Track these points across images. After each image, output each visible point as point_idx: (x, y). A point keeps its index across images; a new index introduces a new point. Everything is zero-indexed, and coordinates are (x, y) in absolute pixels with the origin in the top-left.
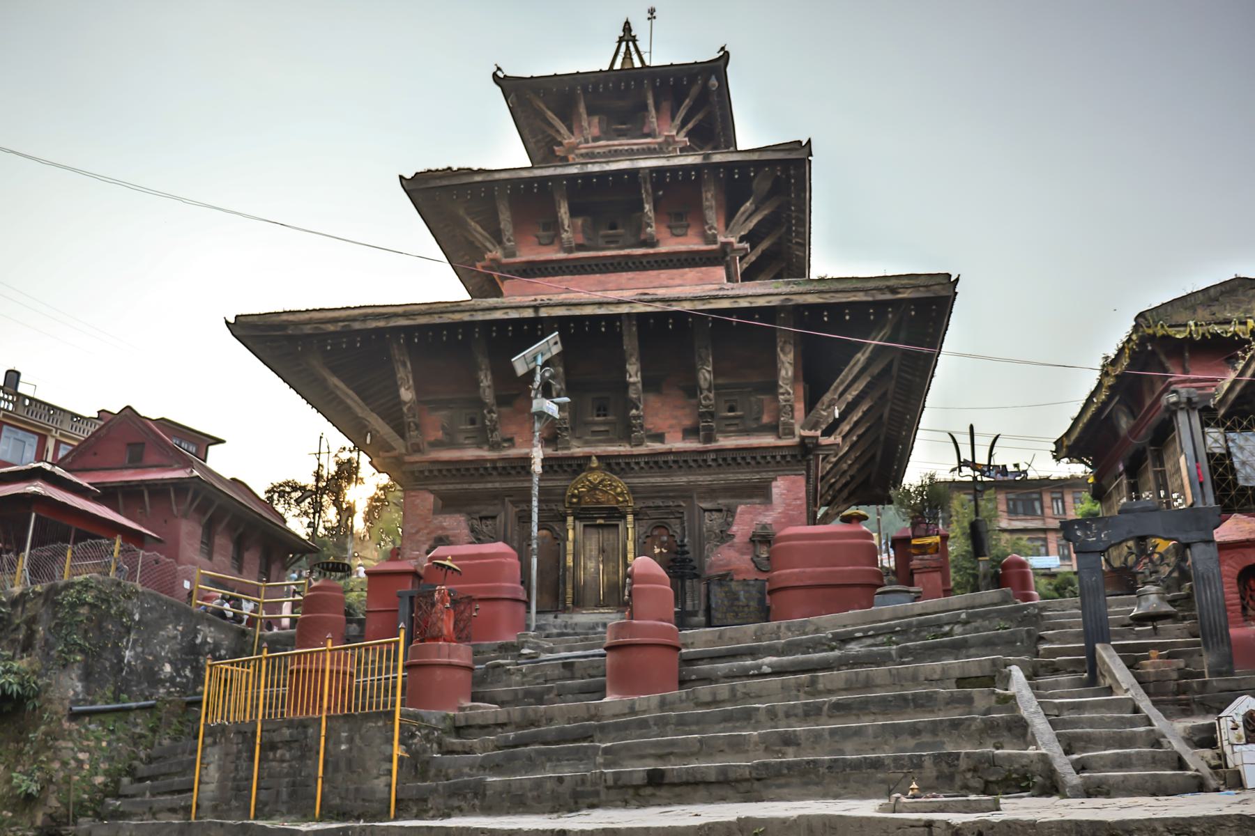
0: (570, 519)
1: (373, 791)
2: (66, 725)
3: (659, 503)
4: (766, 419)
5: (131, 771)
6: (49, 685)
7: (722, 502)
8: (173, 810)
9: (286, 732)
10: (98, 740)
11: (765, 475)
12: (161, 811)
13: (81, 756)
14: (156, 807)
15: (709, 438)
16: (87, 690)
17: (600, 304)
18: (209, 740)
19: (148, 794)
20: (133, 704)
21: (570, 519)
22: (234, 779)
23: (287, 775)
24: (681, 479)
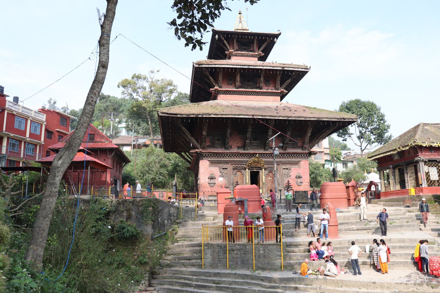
0: (247, 169)
2: (151, 242)
6: (142, 230)
7: (288, 166)
10: (157, 244)
11: (299, 160)
12: (188, 265)
13: (154, 250)
14: (185, 264)
15: (285, 149)
16: (154, 232)
17: (271, 116)
18: (206, 247)
19: (177, 260)
20: (163, 234)
21: (247, 169)
22: (218, 258)
23: (239, 258)
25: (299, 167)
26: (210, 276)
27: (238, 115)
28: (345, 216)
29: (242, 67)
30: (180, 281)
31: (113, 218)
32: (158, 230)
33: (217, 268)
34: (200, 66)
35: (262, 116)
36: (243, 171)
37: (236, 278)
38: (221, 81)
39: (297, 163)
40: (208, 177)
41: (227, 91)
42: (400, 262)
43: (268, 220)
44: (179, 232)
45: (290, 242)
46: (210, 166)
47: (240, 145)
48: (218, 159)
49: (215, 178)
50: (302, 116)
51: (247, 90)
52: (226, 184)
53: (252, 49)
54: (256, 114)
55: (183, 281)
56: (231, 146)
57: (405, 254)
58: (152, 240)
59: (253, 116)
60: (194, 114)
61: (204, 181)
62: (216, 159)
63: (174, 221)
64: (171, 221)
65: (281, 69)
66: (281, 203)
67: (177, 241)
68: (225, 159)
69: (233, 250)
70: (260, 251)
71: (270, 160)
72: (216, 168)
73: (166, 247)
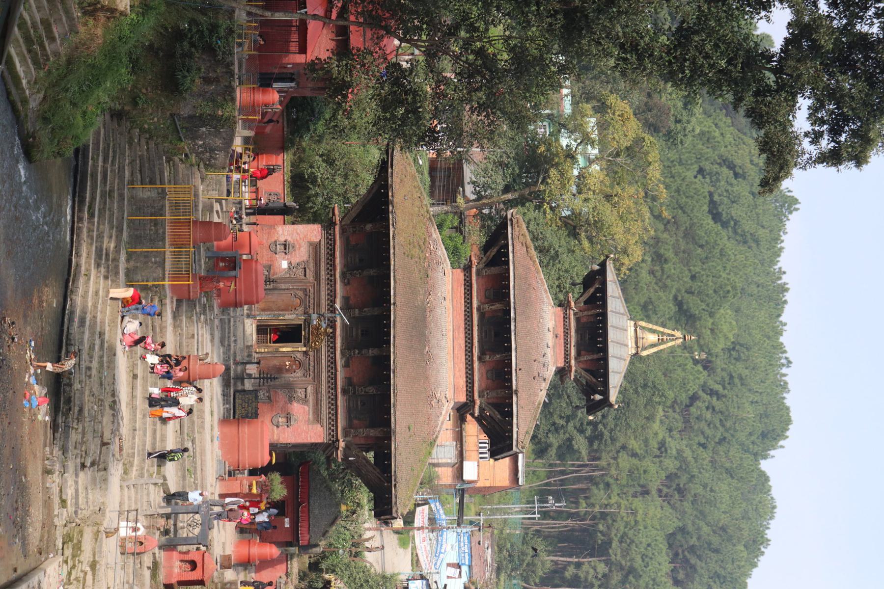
1: (136, 274)
2: (168, 113)
3: (312, 364)
4: (356, 422)
5: (151, 138)
7: (311, 399)
8: (132, 175)
9: (161, 231)
10: (164, 124)
12: (132, 167)
13: (156, 119)
16: (184, 118)
18: (160, 191)
20: (181, 135)
24: (324, 376)
25: (308, 422)
26: (118, 189)
27: (394, 276)
28: (204, 412)
29: (512, 305)
30: (111, 150)
31: (204, 57)
32: (187, 125)
33: (129, 205)
34: (509, 223)
35: (394, 321)
36: (300, 310)
37: (117, 219)
38: (489, 272)
39: (317, 418)
40: (289, 239)
41: (471, 286)
42: (135, 416)
43: (201, 284)
44: (183, 166)
45: (166, 304)
46: (311, 244)
47: (352, 302)
48: (323, 260)
49: (286, 253)
50: (399, 398)
51: (475, 328)
52: (274, 274)
53: (583, 352)
54: (399, 308)
55: (111, 154)
56: (348, 283)
57: (146, 428)
58: (171, 115)
59: (394, 304)
60: (393, 196)
61: (281, 232)
62: (323, 256)
63: (202, 159)
64: (202, 152)
65: (514, 387)
66: (236, 363)
67: (168, 161)
68: (323, 273)
69: (156, 225)
70: (155, 257)
71: (323, 361)
72: (307, 255)
73: (159, 140)
